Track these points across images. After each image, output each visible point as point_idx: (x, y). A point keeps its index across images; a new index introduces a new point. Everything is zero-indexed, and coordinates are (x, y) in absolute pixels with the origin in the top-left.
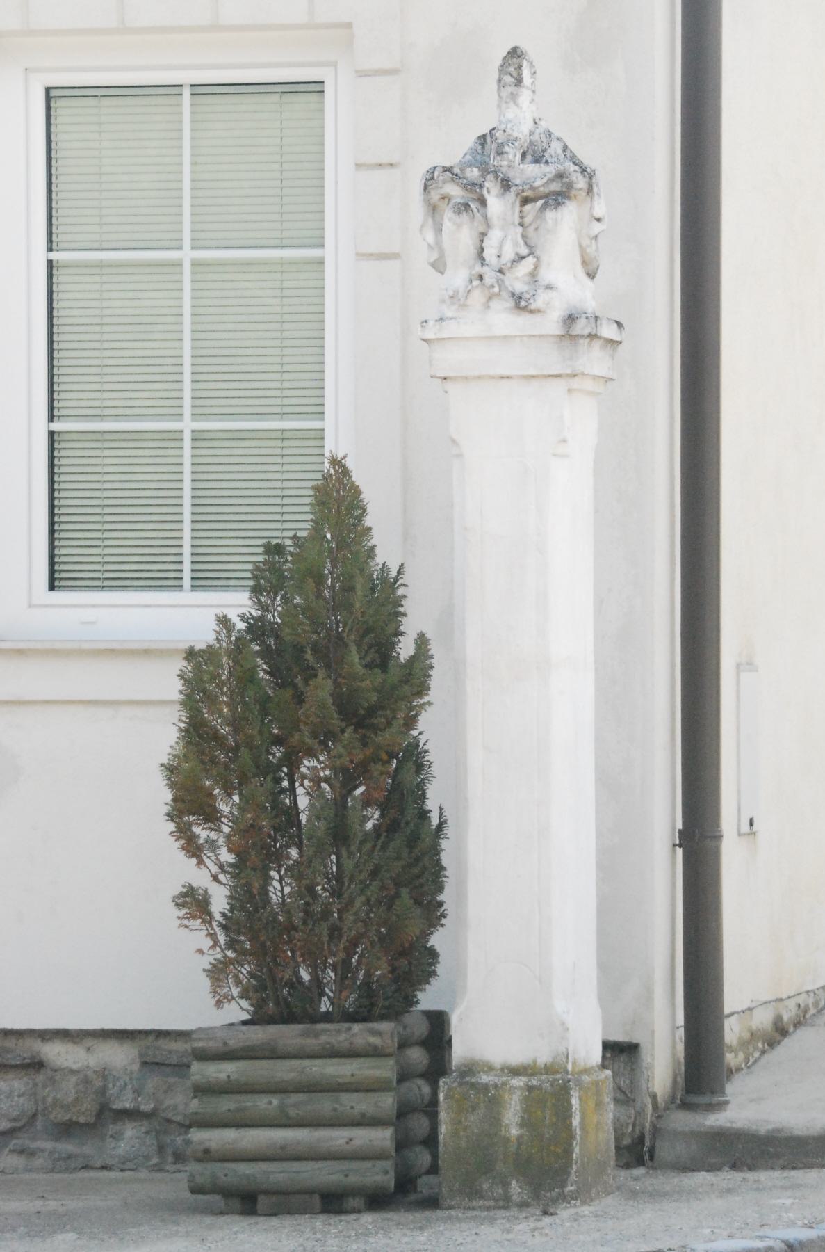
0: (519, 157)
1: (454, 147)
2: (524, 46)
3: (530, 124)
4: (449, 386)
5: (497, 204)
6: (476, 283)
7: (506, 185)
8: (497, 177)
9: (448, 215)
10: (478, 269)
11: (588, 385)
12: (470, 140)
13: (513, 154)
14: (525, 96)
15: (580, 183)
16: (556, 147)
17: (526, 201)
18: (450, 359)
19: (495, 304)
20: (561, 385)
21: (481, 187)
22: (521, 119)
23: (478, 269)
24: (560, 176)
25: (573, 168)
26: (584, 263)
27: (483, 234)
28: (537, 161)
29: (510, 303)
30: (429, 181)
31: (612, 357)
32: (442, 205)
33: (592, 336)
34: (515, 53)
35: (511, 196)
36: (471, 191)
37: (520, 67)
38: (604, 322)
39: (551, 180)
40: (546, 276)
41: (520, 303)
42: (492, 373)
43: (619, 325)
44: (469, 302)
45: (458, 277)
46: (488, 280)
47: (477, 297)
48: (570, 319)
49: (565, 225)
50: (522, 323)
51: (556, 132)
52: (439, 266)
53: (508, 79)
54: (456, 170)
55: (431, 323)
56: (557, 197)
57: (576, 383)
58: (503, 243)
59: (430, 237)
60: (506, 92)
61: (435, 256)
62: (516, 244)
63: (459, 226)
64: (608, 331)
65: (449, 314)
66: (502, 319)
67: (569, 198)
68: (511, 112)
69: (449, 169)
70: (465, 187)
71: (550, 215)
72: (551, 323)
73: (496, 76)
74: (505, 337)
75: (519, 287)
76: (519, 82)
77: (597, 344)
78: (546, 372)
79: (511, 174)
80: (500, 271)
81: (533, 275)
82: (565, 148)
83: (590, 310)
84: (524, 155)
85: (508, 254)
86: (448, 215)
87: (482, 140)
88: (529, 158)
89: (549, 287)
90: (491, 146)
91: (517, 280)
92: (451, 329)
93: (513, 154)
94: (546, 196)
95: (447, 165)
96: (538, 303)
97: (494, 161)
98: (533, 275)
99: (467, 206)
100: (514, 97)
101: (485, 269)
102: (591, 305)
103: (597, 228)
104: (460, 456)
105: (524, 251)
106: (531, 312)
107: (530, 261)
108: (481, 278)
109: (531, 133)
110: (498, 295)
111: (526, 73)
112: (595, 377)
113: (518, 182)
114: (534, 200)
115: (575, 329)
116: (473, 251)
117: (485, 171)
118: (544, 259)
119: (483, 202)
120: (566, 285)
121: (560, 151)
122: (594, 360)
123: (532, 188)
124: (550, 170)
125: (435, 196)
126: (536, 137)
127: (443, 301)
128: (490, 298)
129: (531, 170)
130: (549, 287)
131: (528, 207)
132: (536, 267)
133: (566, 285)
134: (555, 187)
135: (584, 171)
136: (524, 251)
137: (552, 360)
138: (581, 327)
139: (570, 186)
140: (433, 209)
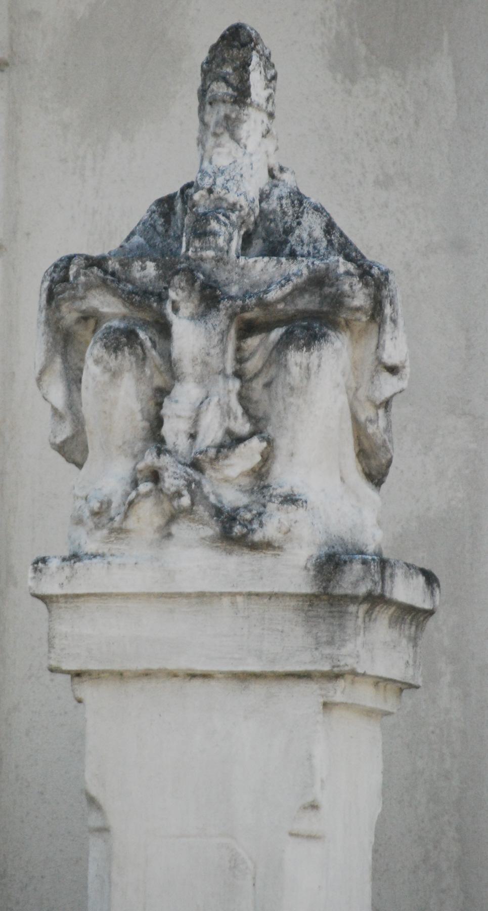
0: (236, 243)
1: (103, 214)
2: (254, 23)
3: (261, 180)
4: (87, 690)
5: (190, 336)
6: (145, 487)
7: (210, 296)
8: (192, 280)
9: (94, 350)
10: (150, 459)
11: (366, 695)
12: (137, 208)
13: (226, 236)
14: (252, 123)
15: (360, 298)
16: (312, 225)
17: (248, 329)
18: (88, 636)
19: (181, 529)
20: (307, 696)
21: (162, 298)
22: (245, 167)
23: (150, 459)
24: (319, 281)
25: (344, 266)
26: (363, 454)
27: (161, 394)
28: (274, 249)
29: (211, 530)
30: (60, 282)
31: (414, 641)
32: (83, 332)
33: (376, 600)
34: (236, 42)
35: (219, 319)
36: (140, 306)
37: (245, 66)
38: (399, 573)
39: (299, 290)
40: (285, 476)
41: (234, 531)
42: (172, 666)
43: (430, 579)
44: (131, 523)
45: (109, 475)
46: (170, 482)
47: (147, 515)
48: (331, 564)
49: (324, 383)
50: (233, 570)
51: (314, 196)
52: (73, 450)
53: (220, 89)
54: (113, 265)
55: (54, 564)
56: (313, 318)
57: (339, 692)
58: (201, 408)
59: (57, 393)
60: (214, 115)
61: (65, 431)
62: (227, 413)
63: (115, 374)
64: (407, 590)
65: (91, 546)
66: (195, 559)
67: (335, 325)
68: (224, 155)
69: (98, 262)
70: (128, 298)
71: (295, 358)
72: (292, 572)
73: (196, 81)
74: (201, 595)
75: (232, 497)
76: (242, 95)
77: (383, 617)
78: (280, 668)
79: (222, 276)
80: (195, 465)
81: (260, 475)
82: (330, 227)
83: (371, 548)
84: (247, 240)
85: (212, 432)
86: (94, 350)
87: (166, 206)
88: (258, 244)
89: (290, 500)
90: (183, 220)
91: (228, 484)
92: (91, 578)
93: (226, 236)
94: (288, 320)
95: (96, 253)
96: (270, 528)
97: (187, 248)
98: (260, 475)
99: (130, 335)
100: (230, 125)
101: (166, 460)
102: (373, 538)
103: (388, 385)
104: (104, 830)
105: (242, 427)
106: (255, 547)
107: (256, 445)
108: (155, 476)
109: (264, 196)
110: (189, 512)
111: (256, 78)
112: (380, 682)
113: (234, 290)
114: (267, 327)
115: (340, 585)
116: (141, 424)
117: (170, 267)
118: (283, 444)
119: (164, 329)
120: (325, 496)
121: (318, 233)
122: (377, 648)
123: (263, 304)
124: (299, 269)
125: (69, 315)
126: (273, 204)
127: (79, 521)
128: (172, 518)
129: (261, 267)
130: (290, 500)
131: (253, 342)
132: (267, 458)
133: (325, 496)
134: (306, 303)
135: (365, 271)
136: (242, 427)
137: (291, 643)
138: (353, 581)
139: (338, 301)
140: (64, 342)
